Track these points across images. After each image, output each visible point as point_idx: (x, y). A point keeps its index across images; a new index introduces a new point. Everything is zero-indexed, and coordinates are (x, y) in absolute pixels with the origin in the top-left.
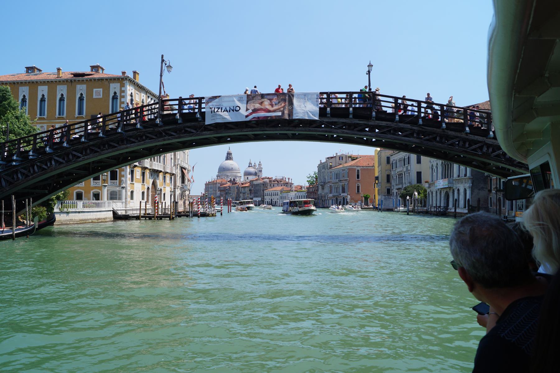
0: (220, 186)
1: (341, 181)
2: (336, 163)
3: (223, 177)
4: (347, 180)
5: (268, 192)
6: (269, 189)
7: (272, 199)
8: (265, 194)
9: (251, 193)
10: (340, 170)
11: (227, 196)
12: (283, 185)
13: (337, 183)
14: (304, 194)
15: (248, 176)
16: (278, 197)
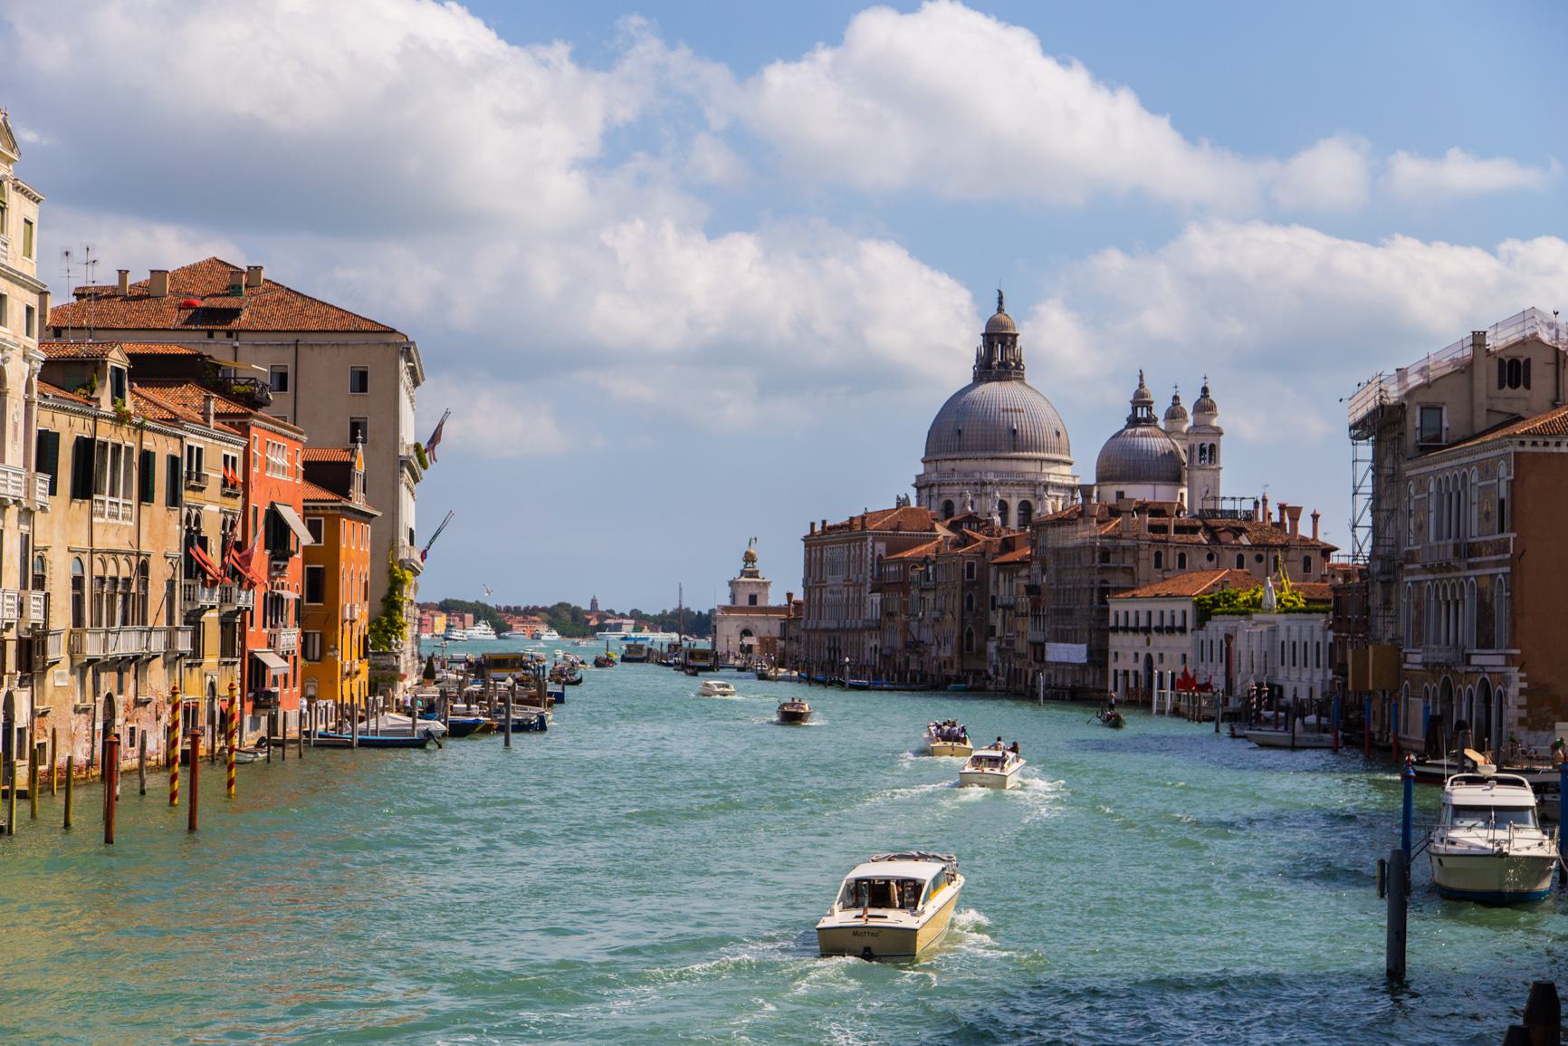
0: (890, 551)
1: (1473, 550)
2: (1472, 412)
3: (956, 489)
4: (1502, 546)
5: (1132, 607)
6: (1149, 582)
7: (1149, 658)
8: (1112, 623)
9: (1036, 606)
10: (1468, 465)
11: (914, 625)
12: (1249, 557)
13: (1448, 567)
14: (1318, 636)
15: (1121, 488)
16: (1185, 642)
